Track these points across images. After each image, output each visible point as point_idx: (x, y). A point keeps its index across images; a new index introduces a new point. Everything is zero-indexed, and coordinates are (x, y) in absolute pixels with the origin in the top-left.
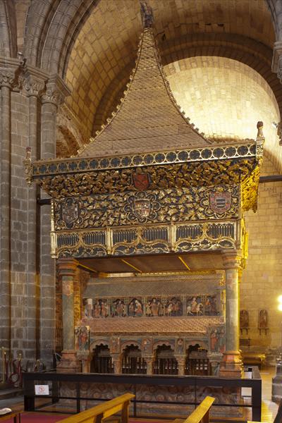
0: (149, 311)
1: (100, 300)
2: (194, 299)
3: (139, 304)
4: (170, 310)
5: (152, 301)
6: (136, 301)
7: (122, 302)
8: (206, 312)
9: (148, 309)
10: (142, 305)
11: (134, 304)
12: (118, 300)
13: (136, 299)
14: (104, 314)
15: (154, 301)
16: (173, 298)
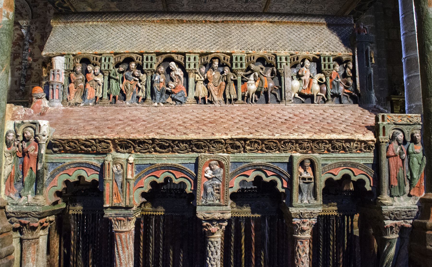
0: (202, 91)
1: (85, 61)
2: (307, 62)
3: (179, 72)
4: (252, 86)
5: (212, 62)
6: (173, 65)
7: (139, 67)
8: (334, 95)
9: (201, 87)
10: (186, 76)
11: (169, 71)
12: (129, 60)
13: (170, 59)
14: (91, 94)
15: (216, 63)
16: (261, 60)
